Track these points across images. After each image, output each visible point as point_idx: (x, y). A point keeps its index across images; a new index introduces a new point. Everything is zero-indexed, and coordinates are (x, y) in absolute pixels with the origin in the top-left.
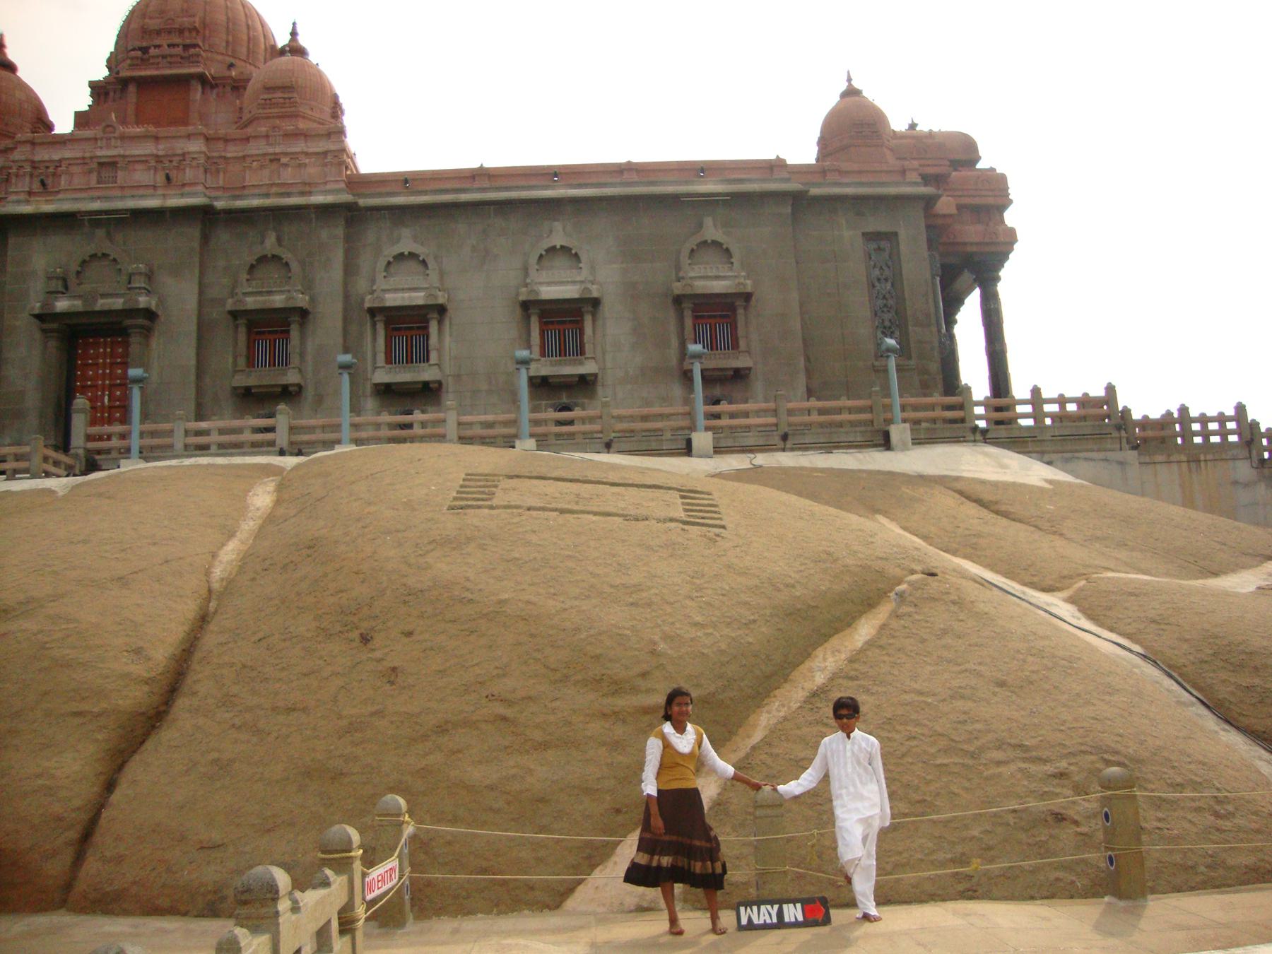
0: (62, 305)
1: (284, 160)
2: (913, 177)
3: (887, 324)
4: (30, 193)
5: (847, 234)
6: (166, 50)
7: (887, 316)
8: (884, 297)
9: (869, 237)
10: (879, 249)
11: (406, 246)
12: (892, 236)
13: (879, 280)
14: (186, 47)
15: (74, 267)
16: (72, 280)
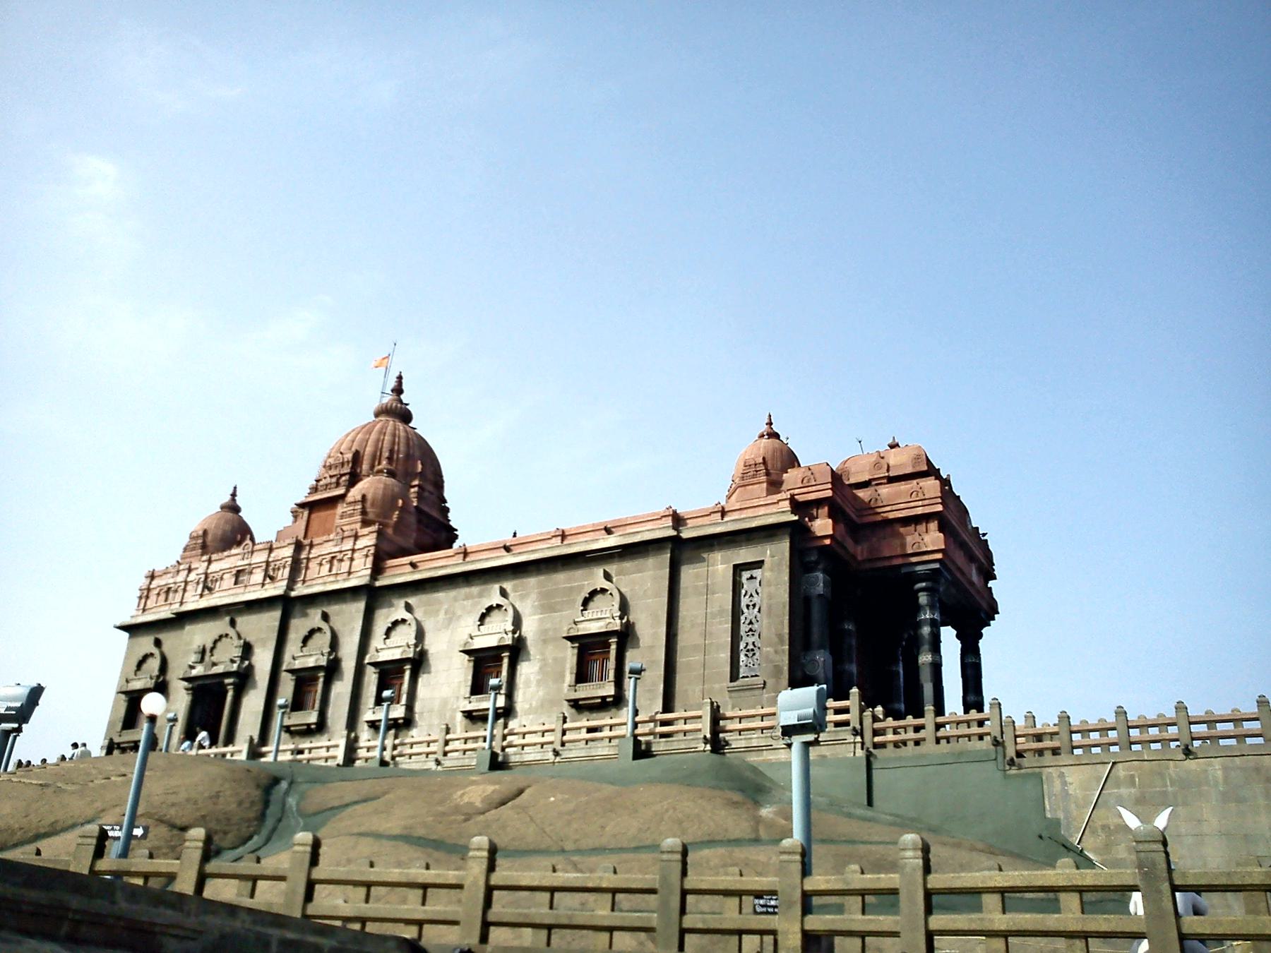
0: (199, 671)
1: (340, 556)
2: (786, 505)
3: (751, 647)
4: (201, 596)
5: (720, 567)
6: (328, 480)
7: (750, 640)
8: (751, 623)
9: (738, 569)
10: (752, 578)
11: (401, 613)
12: (759, 565)
13: (748, 606)
14: (342, 475)
15: (209, 646)
16: (208, 654)
